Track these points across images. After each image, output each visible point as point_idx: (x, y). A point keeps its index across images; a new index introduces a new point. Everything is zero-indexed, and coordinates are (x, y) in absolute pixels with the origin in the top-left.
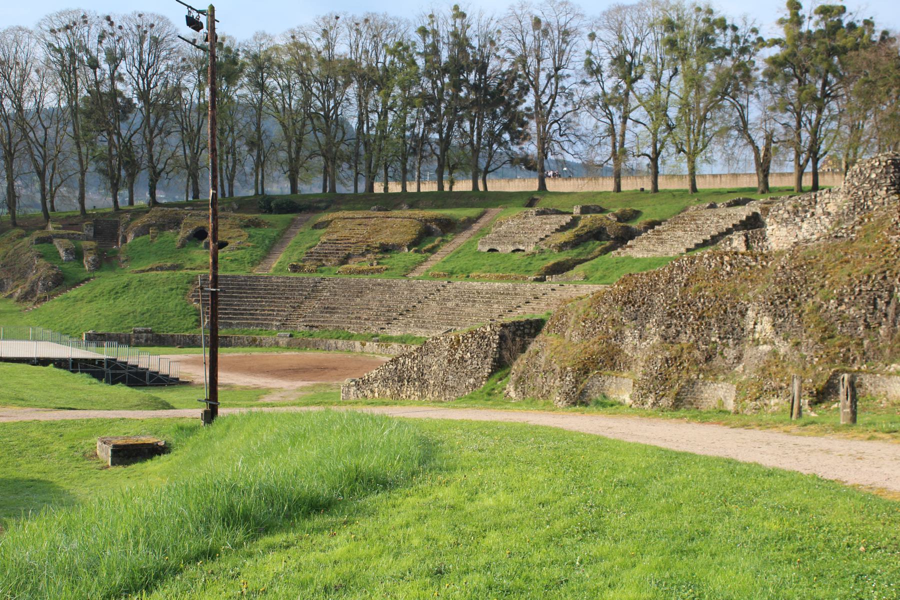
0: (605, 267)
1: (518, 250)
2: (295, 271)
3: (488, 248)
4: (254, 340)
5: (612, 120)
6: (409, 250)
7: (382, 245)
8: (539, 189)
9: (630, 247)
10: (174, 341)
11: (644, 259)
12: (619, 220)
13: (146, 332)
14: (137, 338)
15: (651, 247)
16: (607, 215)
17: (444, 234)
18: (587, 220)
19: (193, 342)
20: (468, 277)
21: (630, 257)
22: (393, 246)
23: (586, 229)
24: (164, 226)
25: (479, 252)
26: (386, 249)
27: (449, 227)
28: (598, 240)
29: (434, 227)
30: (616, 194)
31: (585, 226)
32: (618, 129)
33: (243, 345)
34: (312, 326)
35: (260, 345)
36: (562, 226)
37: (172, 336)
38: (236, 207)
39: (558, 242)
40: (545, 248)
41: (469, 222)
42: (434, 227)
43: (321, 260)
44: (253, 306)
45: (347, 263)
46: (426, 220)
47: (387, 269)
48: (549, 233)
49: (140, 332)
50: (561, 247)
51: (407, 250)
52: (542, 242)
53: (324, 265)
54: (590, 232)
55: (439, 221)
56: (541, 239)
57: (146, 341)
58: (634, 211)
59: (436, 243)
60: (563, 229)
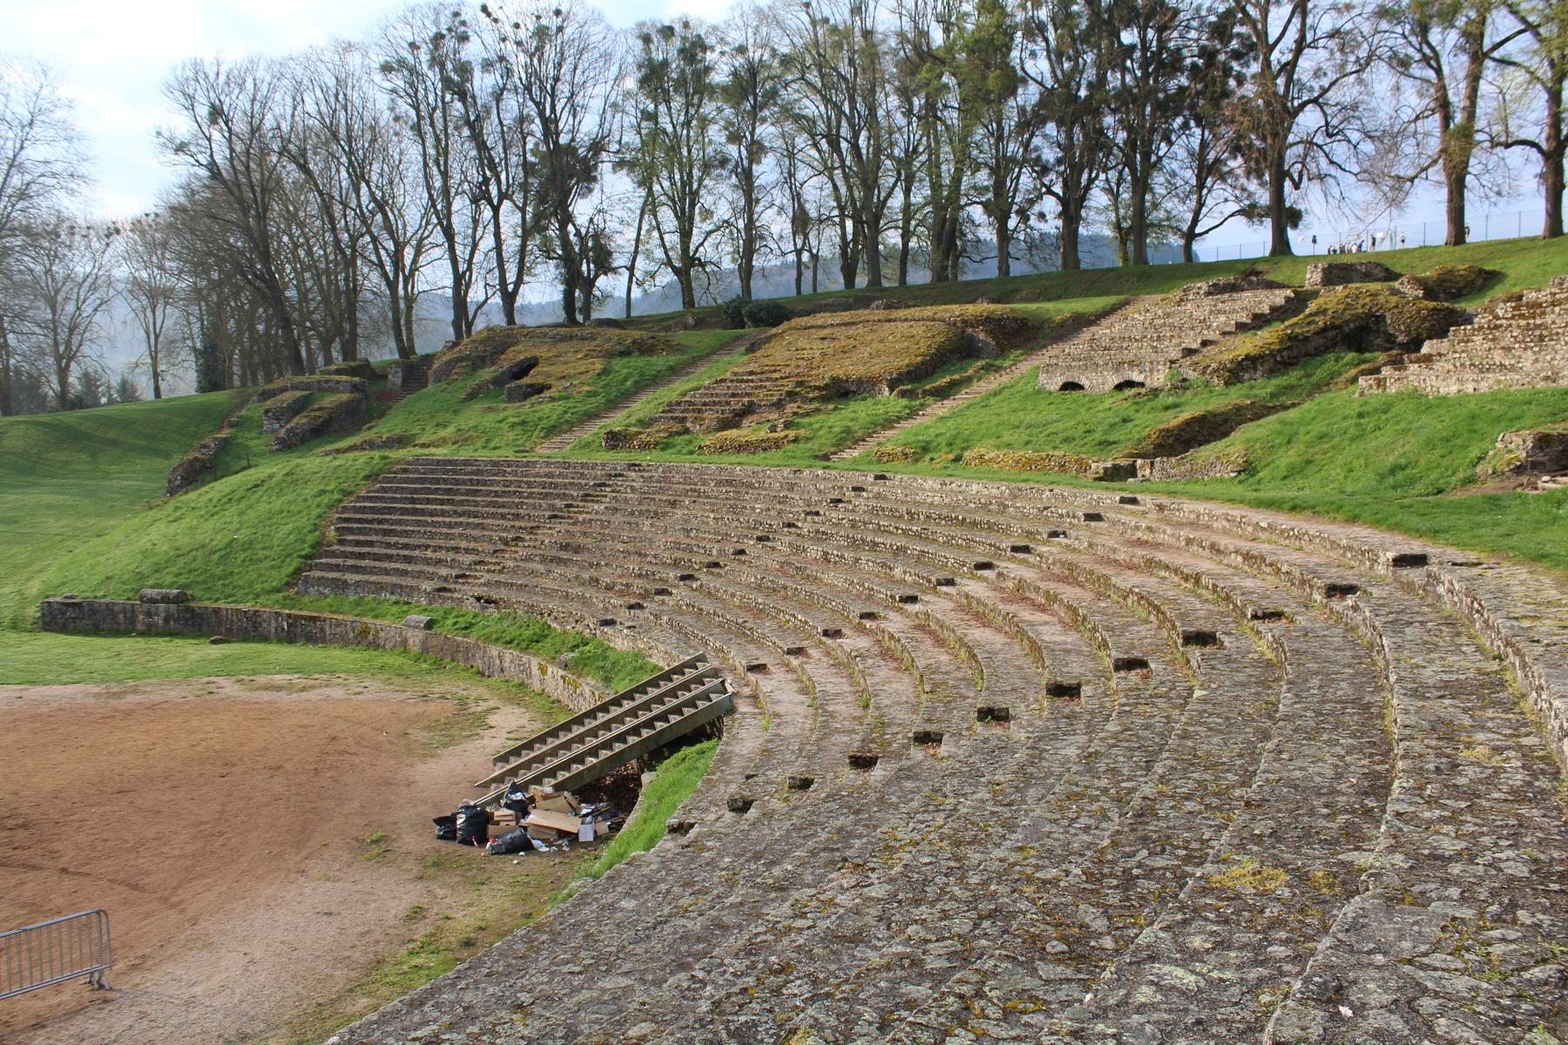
0: (1316, 429)
1: (1129, 384)
2: (614, 447)
3: (1060, 381)
4: (365, 632)
5: (1439, 71)
6: (892, 390)
7: (836, 381)
8: (1274, 252)
9: (1428, 359)
10: (220, 624)
11: (1462, 398)
12: (1430, 293)
13: (165, 599)
14: (149, 614)
15: (1498, 357)
16: (1396, 284)
17: (1002, 351)
18: (1333, 299)
19: (256, 625)
20: (958, 459)
21: (1416, 394)
22: (859, 381)
23: (1321, 321)
24: (483, 359)
25: (1039, 392)
26: (840, 392)
27: (1021, 336)
28: (1350, 348)
29: (982, 336)
30: (1451, 248)
31: (1321, 312)
32: (1457, 96)
33: (345, 643)
34: (489, 601)
35: (375, 645)
36: (1256, 317)
37: (217, 611)
38: (691, 321)
39: (1226, 357)
40: (1192, 375)
41: (1081, 322)
42: (982, 336)
43: (684, 419)
44: (432, 536)
45: (737, 426)
46: (965, 322)
47: (796, 440)
48: (1210, 335)
49: (152, 601)
50: (1236, 372)
51: (886, 392)
52: (1188, 361)
53: (687, 431)
54: (1333, 327)
55: (994, 325)
56: (1189, 352)
57: (166, 620)
58: (1481, 271)
59: (970, 372)
60: (1259, 321)
